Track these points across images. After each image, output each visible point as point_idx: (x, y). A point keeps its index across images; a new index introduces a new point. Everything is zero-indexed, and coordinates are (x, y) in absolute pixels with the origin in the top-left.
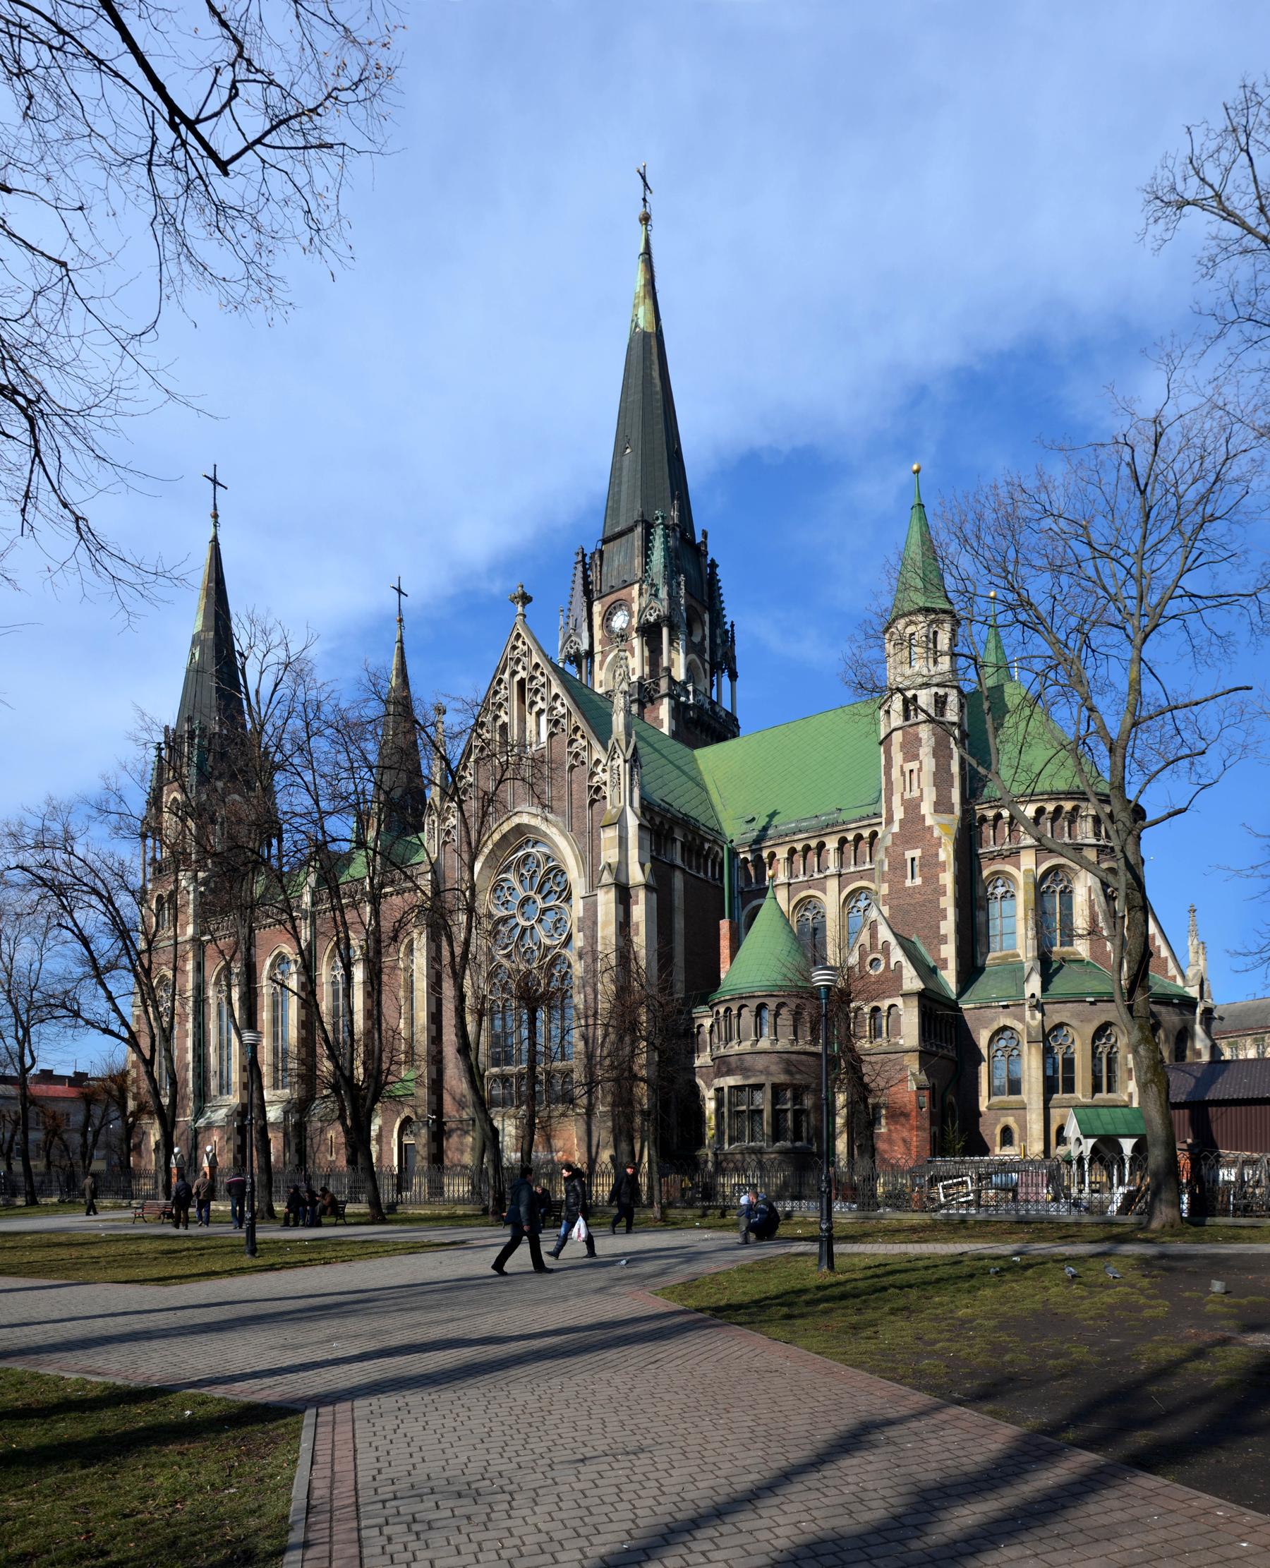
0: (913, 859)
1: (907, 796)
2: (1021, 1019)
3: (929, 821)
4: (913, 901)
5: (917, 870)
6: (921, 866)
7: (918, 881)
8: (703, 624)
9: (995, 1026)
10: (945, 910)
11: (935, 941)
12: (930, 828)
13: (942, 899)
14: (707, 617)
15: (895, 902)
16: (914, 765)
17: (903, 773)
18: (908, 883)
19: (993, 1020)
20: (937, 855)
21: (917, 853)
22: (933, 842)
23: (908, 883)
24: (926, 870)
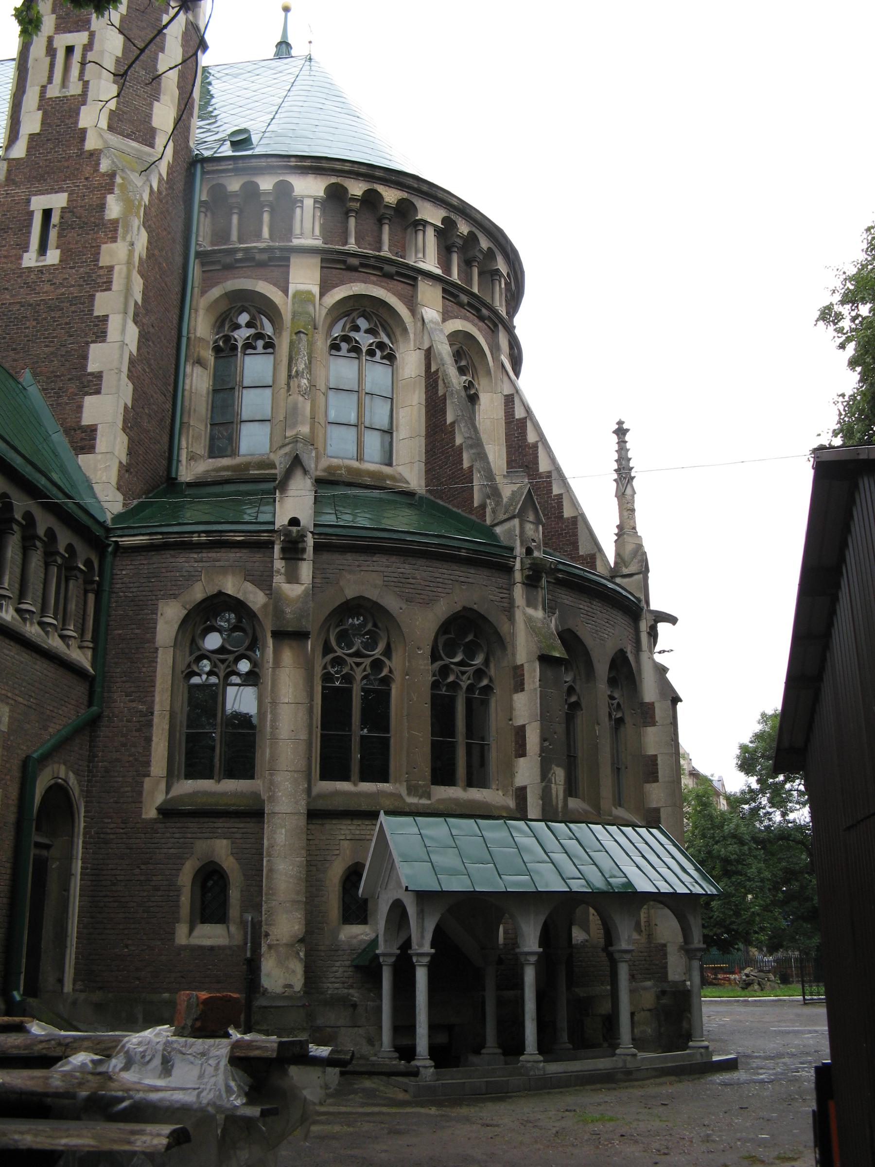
0: (47, 214)
1: (54, 91)
2: (264, 581)
3: (91, 144)
4: (32, 299)
5: (53, 234)
6: (63, 226)
7: (53, 256)
9: (198, 593)
10: (105, 319)
11: (72, 387)
12: (94, 156)
13: (100, 296)
16: (79, 39)
17: (51, 51)
18: (30, 259)
19: (191, 578)
20: (102, 207)
21: (58, 201)
22: (97, 180)
23: (30, 259)
24: (72, 235)
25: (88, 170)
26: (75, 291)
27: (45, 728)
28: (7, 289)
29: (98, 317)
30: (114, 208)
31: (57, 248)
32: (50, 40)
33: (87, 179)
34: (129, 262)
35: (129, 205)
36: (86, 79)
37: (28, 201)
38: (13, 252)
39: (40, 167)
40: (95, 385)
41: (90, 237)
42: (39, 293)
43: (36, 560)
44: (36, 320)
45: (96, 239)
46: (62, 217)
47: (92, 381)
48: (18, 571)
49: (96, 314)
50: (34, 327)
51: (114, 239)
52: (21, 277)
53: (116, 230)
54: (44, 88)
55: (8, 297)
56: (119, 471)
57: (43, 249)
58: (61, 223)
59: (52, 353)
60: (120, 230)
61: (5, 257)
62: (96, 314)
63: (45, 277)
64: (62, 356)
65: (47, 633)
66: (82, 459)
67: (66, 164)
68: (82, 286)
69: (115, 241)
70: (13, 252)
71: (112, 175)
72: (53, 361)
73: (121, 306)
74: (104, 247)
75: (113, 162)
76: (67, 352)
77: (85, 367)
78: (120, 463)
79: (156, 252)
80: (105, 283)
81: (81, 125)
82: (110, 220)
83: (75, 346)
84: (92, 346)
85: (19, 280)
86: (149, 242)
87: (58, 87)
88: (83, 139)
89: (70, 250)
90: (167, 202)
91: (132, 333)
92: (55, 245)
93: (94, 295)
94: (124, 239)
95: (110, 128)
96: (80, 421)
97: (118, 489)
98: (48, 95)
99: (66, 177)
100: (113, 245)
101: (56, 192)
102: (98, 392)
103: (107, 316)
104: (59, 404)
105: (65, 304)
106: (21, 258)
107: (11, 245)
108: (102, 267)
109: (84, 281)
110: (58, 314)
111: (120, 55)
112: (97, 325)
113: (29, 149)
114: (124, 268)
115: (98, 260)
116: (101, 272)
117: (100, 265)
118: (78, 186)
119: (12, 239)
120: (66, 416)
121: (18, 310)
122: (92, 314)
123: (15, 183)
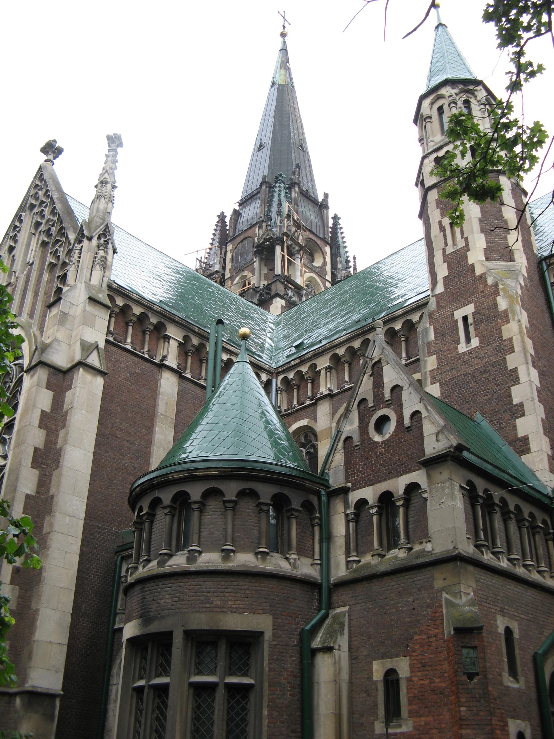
0: (465, 319)
1: (450, 250)
4: (470, 370)
5: (472, 329)
6: (477, 323)
7: (475, 342)
8: (324, 255)
10: (516, 370)
11: (507, 416)
12: (483, 277)
13: (508, 357)
14: (328, 249)
15: (448, 377)
18: (462, 348)
20: (495, 305)
21: (469, 310)
23: (462, 348)
25: (481, 287)
26: (493, 359)
27: (542, 633)
28: (454, 368)
29: (511, 370)
30: (502, 304)
31: (476, 337)
32: (440, 223)
33: (482, 292)
34: (521, 332)
35: (511, 299)
36: (465, 237)
37: (453, 315)
38: (452, 346)
39: (454, 294)
40: (520, 411)
41: (494, 324)
42: (473, 366)
43: (513, 526)
44: (475, 381)
45: (497, 325)
46: (474, 318)
47: (518, 409)
48: (503, 535)
49: (509, 368)
50: (475, 386)
51: (508, 322)
52: (459, 359)
53: (507, 316)
54: (444, 250)
55: (455, 373)
56: (549, 460)
57: (468, 340)
58: (474, 322)
59: (490, 399)
60: (510, 315)
61: (448, 350)
62: (509, 368)
63: (474, 355)
64: (496, 399)
65: (529, 571)
66: (524, 458)
67: (468, 287)
68: (496, 354)
69: (509, 323)
70: (452, 346)
71: (496, 285)
72: (491, 403)
73: (523, 360)
74: (503, 328)
75: (495, 277)
76: (498, 396)
77: (511, 402)
78: (548, 455)
79: (535, 321)
80: (509, 349)
81: (470, 263)
82: (502, 311)
83: (502, 391)
84: (512, 388)
85: (459, 361)
86: (529, 317)
87: (452, 246)
88: (473, 270)
89: (484, 336)
90: (532, 290)
91: (534, 373)
92: (474, 335)
93: (505, 358)
94: (514, 319)
95: (487, 259)
96: (517, 435)
97: (551, 472)
98: (447, 253)
99: (470, 295)
100: (508, 325)
101: (467, 305)
102: (523, 415)
103: (517, 368)
104: (501, 428)
105: (490, 368)
106: (457, 348)
107: (449, 343)
108: (505, 340)
109: (497, 351)
110: (486, 375)
111: (480, 217)
112: (512, 375)
113: (445, 286)
114: (519, 336)
115: (502, 337)
116: (506, 343)
117: (504, 339)
118: (478, 297)
119: (449, 339)
120: (507, 434)
121: (463, 379)
122: (507, 369)
123: (442, 307)
